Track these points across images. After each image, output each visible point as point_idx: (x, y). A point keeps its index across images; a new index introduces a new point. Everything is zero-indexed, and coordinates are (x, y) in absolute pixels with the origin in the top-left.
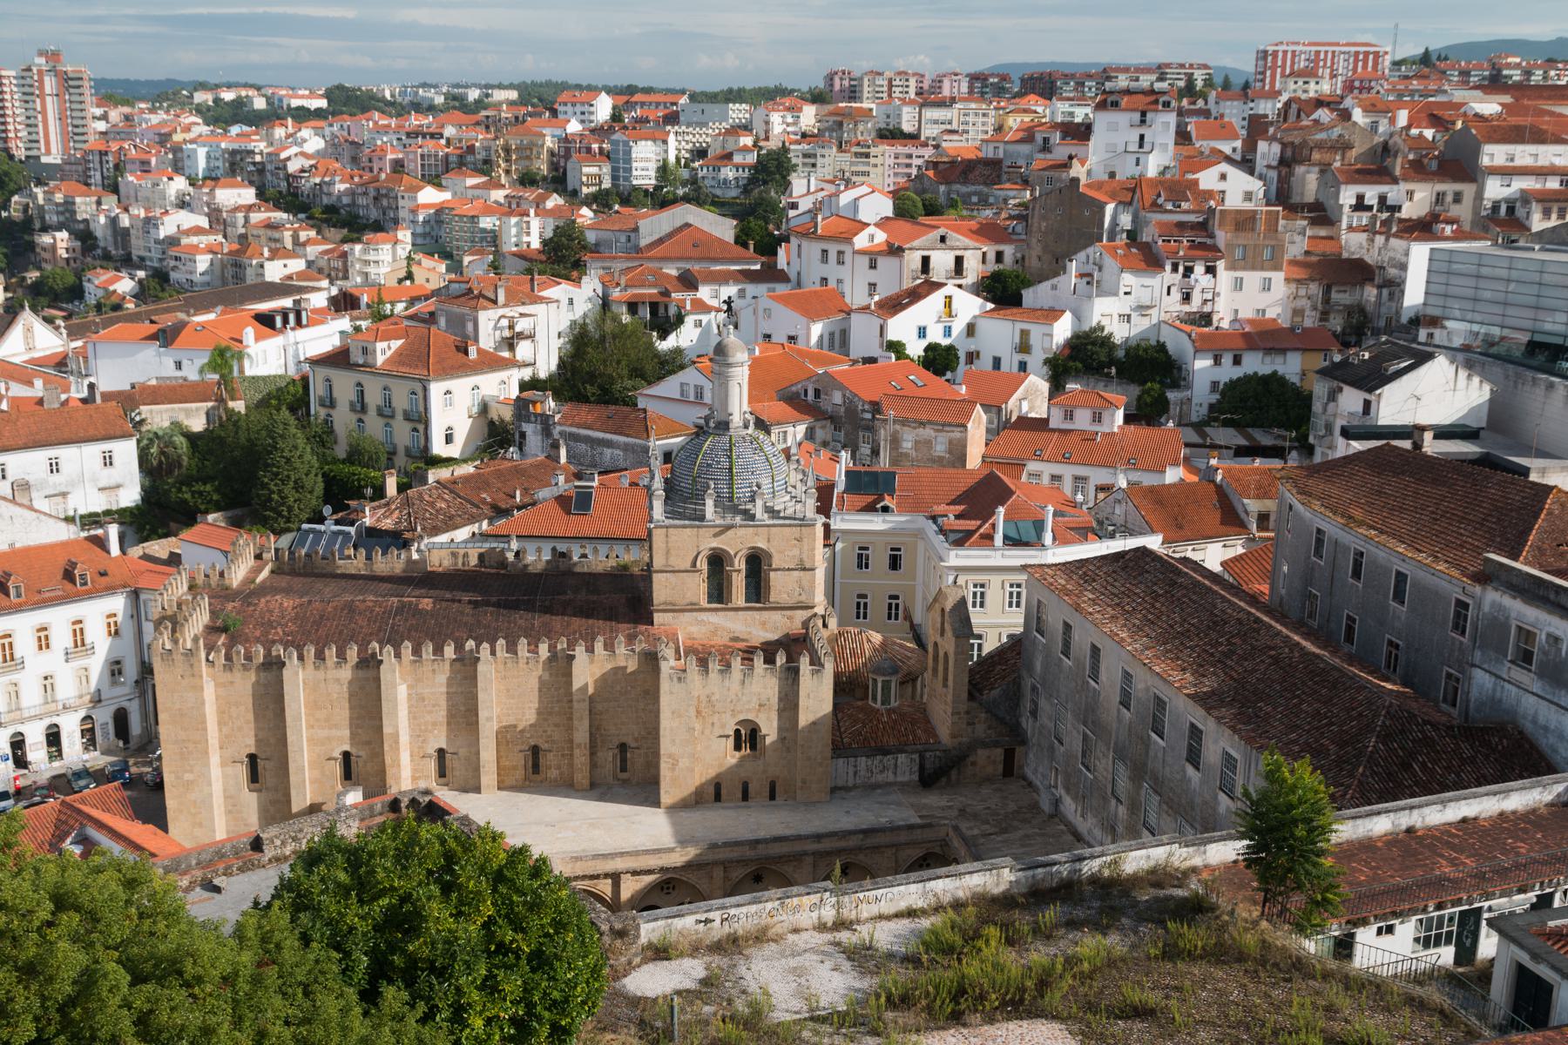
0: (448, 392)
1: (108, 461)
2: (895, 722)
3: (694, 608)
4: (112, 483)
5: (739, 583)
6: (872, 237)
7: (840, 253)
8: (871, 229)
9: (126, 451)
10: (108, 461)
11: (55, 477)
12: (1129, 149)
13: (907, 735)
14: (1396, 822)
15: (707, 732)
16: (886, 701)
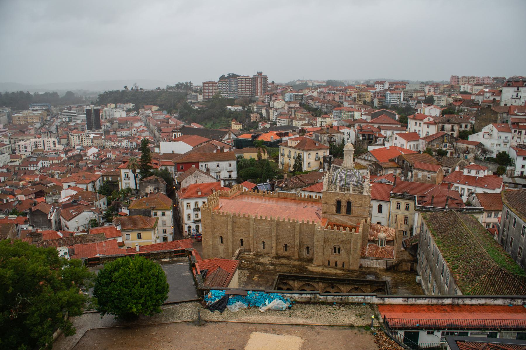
0: (309, 154)
1: (230, 165)
2: (383, 251)
3: (332, 214)
4: (230, 170)
5: (344, 209)
6: (429, 119)
7: (420, 123)
8: (429, 117)
9: (234, 163)
10: (230, 165)
11: (218, 168)
12: (513, 97)
13: (385, 255)
14: (453, 301)
15: (327, 247)
16: (381, 245)
